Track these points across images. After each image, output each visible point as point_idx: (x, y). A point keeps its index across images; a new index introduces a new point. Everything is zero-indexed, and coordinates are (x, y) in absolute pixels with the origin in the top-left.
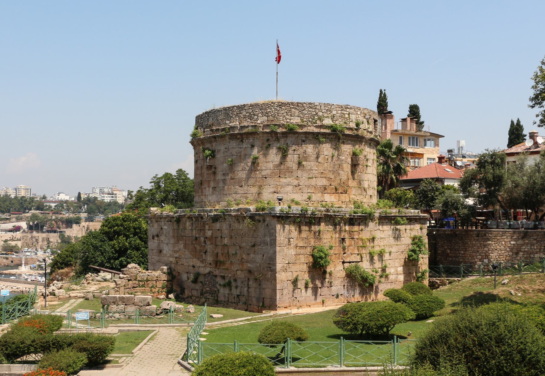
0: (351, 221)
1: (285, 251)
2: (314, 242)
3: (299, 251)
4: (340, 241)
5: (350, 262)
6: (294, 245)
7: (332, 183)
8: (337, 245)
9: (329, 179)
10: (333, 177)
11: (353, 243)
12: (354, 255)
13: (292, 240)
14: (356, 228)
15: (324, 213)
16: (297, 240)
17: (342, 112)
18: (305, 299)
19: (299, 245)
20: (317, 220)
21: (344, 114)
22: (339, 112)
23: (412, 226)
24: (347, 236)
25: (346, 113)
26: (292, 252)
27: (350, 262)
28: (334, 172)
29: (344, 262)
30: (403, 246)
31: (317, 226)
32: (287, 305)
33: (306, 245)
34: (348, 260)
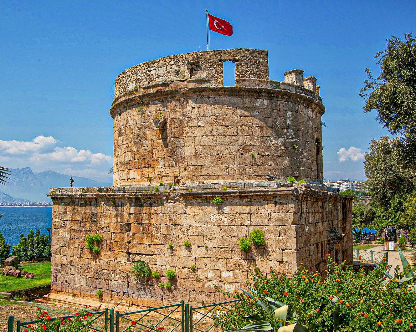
0: (138, 202)
1: (60, 234)
2: (91, 226)
3: (74, 234)
4: (121, 226)
5: (138, 254)
6: (69, 227)
7: (136, 157)
8: (119, 231)
9: (133, 153)
10: (136, 149)
11: (141, 229)
12: (143, 245)
13: (66, 222)
14: (145, 210)
15: (97, 193)
16: (71, 222)
17: (149, 69)
18: (78, 287)
19: (73, 228)
20: (94, 202)
21: (150, 71)
22: (144, 71)
23: (255, 208)
24: (132, 220)
25: (152, 69)
26: (66, 235)
27: (138, 254)
28: (136, 143)
29: (129, 254)
30: (235, 239)
31: (93, 208)
32: (60, 289)
33: (81, 229)
34: (134, 250)
